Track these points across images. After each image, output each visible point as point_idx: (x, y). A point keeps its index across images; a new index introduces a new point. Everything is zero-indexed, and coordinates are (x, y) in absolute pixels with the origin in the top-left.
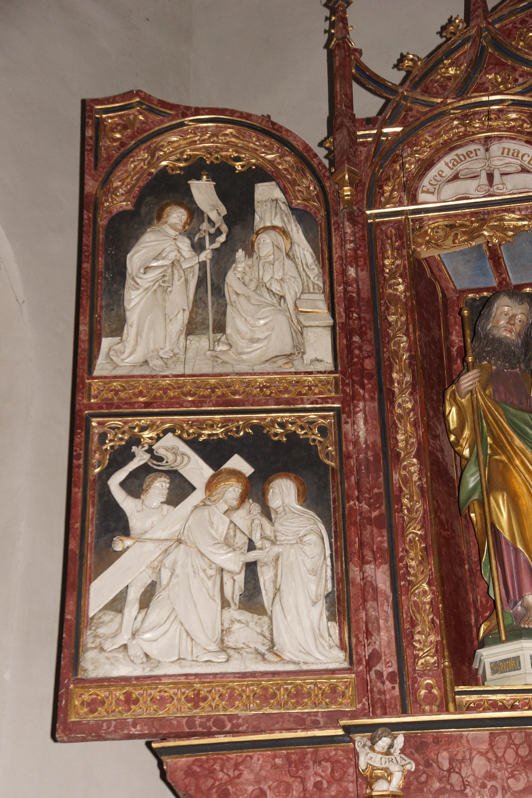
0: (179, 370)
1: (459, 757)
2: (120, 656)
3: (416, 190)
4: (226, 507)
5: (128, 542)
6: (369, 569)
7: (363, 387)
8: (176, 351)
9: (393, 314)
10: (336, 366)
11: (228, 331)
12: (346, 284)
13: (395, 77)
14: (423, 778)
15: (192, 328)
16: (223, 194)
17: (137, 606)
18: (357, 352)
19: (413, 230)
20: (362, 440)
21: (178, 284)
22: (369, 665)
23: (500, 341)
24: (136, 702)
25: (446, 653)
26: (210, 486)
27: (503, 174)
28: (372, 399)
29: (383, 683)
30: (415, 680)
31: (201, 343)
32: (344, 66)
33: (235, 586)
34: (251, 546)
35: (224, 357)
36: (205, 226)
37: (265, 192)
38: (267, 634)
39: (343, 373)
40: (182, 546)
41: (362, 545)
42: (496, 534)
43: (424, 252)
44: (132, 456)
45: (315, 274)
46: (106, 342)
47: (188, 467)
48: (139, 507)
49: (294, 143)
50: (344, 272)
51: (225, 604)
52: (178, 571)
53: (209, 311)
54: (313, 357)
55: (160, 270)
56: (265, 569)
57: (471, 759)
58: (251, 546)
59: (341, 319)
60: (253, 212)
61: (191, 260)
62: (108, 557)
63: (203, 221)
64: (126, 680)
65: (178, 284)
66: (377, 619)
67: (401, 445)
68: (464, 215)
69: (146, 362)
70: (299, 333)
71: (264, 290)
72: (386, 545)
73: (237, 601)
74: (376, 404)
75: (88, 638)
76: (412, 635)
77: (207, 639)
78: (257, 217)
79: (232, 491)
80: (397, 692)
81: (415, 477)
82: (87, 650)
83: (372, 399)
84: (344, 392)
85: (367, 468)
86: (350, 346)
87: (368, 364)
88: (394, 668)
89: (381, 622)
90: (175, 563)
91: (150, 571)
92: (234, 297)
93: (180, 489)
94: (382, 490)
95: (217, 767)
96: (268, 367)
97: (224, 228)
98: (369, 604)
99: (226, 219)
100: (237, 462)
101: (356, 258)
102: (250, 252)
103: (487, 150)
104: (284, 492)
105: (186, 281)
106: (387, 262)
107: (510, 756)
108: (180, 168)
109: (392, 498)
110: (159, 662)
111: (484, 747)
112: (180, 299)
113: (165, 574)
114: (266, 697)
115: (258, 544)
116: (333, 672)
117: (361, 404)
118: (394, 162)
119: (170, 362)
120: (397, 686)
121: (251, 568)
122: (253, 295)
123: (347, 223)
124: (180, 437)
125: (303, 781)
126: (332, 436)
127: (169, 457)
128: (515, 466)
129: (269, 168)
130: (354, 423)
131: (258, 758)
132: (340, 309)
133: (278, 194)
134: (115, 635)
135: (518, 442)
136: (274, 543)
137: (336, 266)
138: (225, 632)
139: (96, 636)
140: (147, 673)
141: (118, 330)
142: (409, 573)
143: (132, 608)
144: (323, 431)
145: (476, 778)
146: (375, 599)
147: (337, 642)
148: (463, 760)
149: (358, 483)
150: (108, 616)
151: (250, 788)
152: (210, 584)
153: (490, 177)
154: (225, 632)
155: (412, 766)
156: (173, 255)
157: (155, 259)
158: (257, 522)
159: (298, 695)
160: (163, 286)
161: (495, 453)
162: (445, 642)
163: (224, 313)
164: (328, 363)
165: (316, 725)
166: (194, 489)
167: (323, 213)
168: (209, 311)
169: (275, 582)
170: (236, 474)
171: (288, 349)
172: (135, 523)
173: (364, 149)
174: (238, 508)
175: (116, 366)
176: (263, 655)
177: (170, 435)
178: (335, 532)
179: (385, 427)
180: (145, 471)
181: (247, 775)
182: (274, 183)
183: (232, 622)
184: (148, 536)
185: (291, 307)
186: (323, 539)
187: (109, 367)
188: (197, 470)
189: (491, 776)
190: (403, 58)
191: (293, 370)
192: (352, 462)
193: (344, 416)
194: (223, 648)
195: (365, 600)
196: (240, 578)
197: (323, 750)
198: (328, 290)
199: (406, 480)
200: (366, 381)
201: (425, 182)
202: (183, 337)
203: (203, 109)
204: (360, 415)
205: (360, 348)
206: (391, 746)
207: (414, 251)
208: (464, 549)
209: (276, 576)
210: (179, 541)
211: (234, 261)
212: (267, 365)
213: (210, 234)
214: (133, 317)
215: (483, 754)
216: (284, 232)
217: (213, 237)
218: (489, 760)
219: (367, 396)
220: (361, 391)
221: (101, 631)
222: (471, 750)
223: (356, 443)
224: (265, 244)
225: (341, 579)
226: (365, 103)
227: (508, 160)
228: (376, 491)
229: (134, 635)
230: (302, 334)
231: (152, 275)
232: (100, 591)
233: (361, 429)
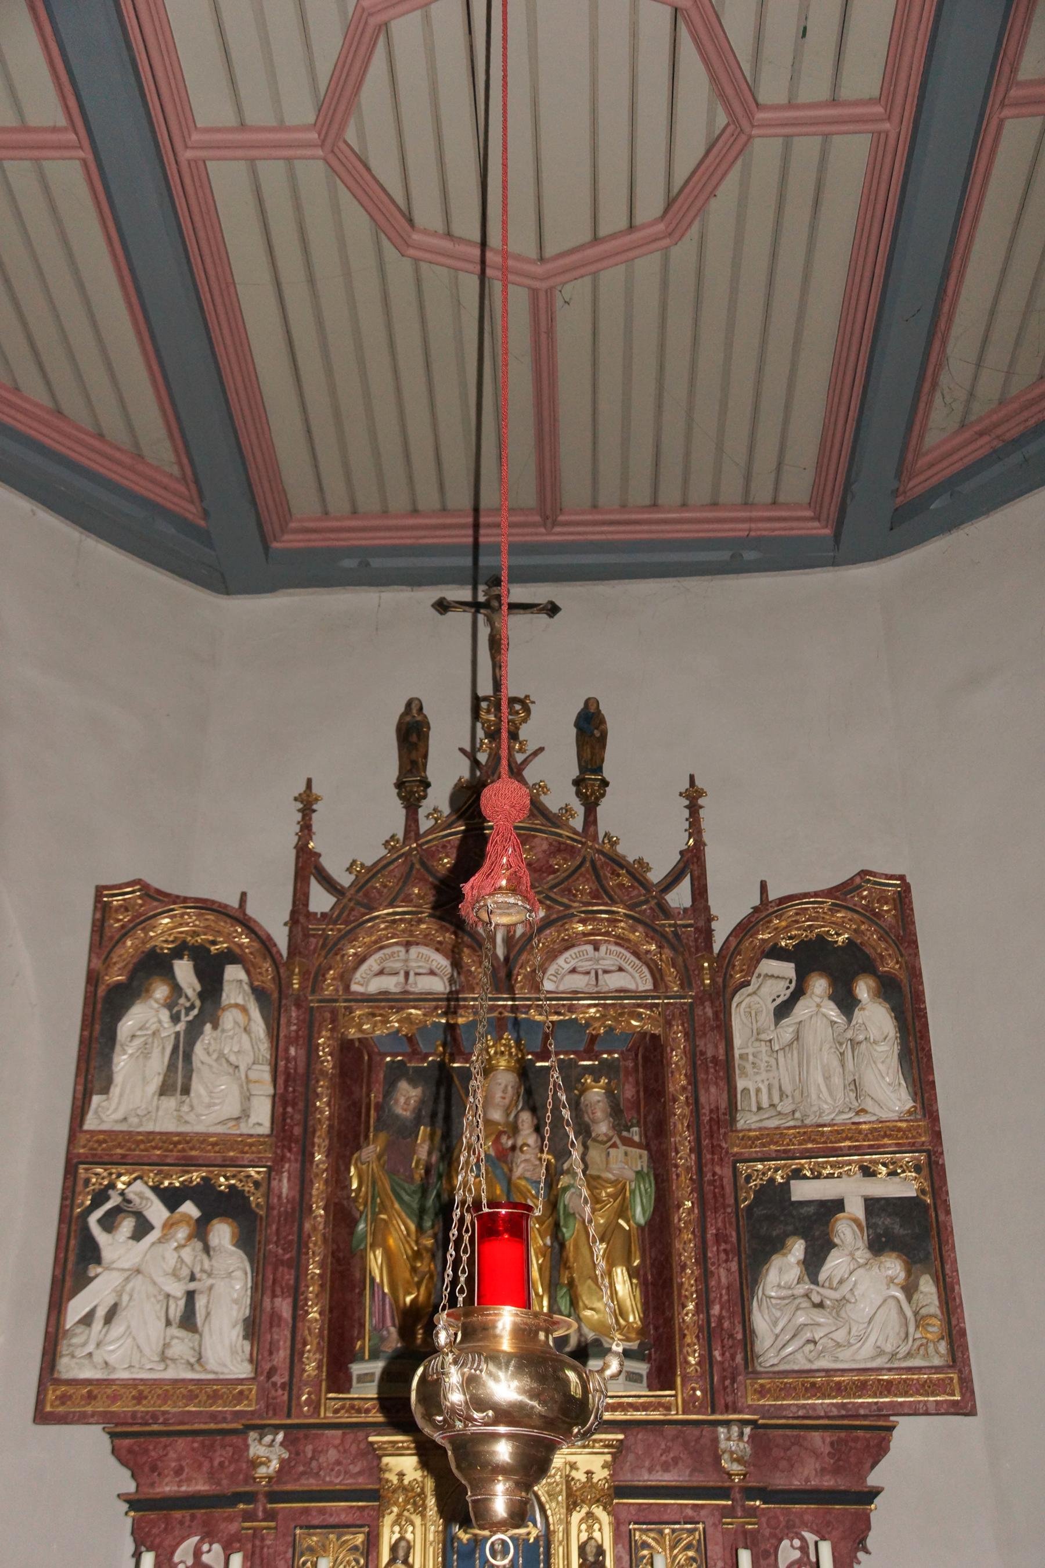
0: (149, 1127)
1: (320, 1449)
2: (86, 1362)
3: (350, 980)
4: (175, 1244)
5: (99, 1270)
6: (278, 1301)
7: (290, 1150)
8: (150, 1109)
9: (321, 1087)
10: (272, 1129)
11: (192, 1094)
12: (288, 1060)
13: (345, 880)
14: (293, 1464)
15: (165, 1090)
16: (199, 973)
17: (102, 1322)
18: (288, 1121)
19: (344, 1015)
20: (284, 1195)
21: (156, 1052)
22: (269, 1376)
23: (397, 1117)
24: (95, 1398)
25: (324, 1369)
26: (168, 1225)
27: (417, 974)
28: (296, 1160)
29: (276, 1391)
30: (300, 1389)
31: (170, 1103)
32: (307, 866)
33: (177, 1309)
34: (193, 1278)
35: (187, 1118)
36: (182, 1001)
37: (234, 973)
38: (197, 1348)
39: (276, 1137)
40: (140, 1277)
41: (274, 1281)
42: (373, 1279)
43: (352, 1033)
44: (108, 1198)
45: (264, 1048)
46: (96, 1099)
47: (151, 1209)
48: (110, 1241)
49: (260, 933)
50: (287, 1050)
51: (168, 1323)
52: (135, 1296)
53: (178, 1080)
54: (255, 1121)
55: (142, 1039)
56: (201, 1296)
57: (327, 1451)
58: (193, 1278)
59: (280, 1091)
60: (221, 990)
61: (169, 1030)
62: (83, 1281)
63: (180, 997)
64: (88, 1382)
65: (156, 1052)
66: (278, 1341)
67: (314, 1200)
68: (383, 1008)
69: (125, 1119)
70: (247, 1098)
71: (224, 1060)
72: (292, 1282)
73: (178, 1319)
74: (298, 1165)
75: (64, 1347)
76: (302, 1353)
77: (151, 1351)
78: (224, 995)
79: (182, 1233)
80: (286, 1397)
81: (321, 1227)
82: (61, 1357)
83: (296, 1160)
84: (275, 1153)
85: (285, 1219)
86: (285, 1113)
87: (297, 1131)
88: (286, 1379)
89: (281, 1343)
90: (133, 1290)
91: (114, 1294)
92: (199, 1065)
93: (143, 1227)
94: (295, 1238)
95: (151, 1447)
96: (220, 1129)
97: (198, 1003)
98: (274, 1329)
99: (201, 995)
100: (189, 1209)
101: (297, 1037)
102: (215, 1027)
103: (407, 951)
104: (222, 1233)
105: (164, 1048)
106: (321, 1041)
107: (354, 1449)
108: (168, 949)
109: (302, 1244)
110: (115, 1368)
111: (337, 1442)
112: (158, 1063)
113: (125, 1298)
114: (191, 1397)
115: (198, 1276)
116: (240, 1381)
117: (287, 1166)
118: (337, 954)
119: (144, 1119)
120: (286, 1393)
121: (190, 1295)
122: (214, 1064)
123: (293, 1008)
124: (146, 1183)
125: (211, 1460)
126: (263, 1189)
127: (137, 1200)
128: (393, 1225)
129: (237, 950)
130: (280, 1180)
131: (181, 1443)
132: (281, 1081)
133: (243, 976)
134: (84, 1345)
135: (397, 1206)
136: (210, 1275)
137: (282, 1044)
138: (166, 1346)
139: (70, 1345)
140: (105, 1377)
141: (105, 1090)
142: (306, 1305)
143: (98, 1324)
144: (257, 1184)
145: (328, 1465)
146: (279, 1326)
147: (248, 1356)
148: (321, 1452)
149: (278, 1230)
150: (80, 1329)
151: (173, 1464)
152: (158, 1307)
153: (407, 974)
154: (166, 1346)
155: (286, 1455)
156: (154, 1027)
157: (140, 1029)
158: (199, 1258)
159: (215, 1397)
160: (145, 1052)
161: (380, 1212)
162: (325, 1360)
163: (190, 1078)
164: (265, 1129)
165: (224, 1420)
166: (152, 1228)
167: (275, 995)
168: (178, 1080)
169: (207, 1307)
170: (186, 1218)
171: (236, 1114)
172: (107, 1254)
173: (313, 940)
174: (184, 1246)
175: (103, 1121)
176: (192, 1365)
177: (139, 1182)
178: (257, 1268)
179: (303, 1184)
180: (116, 1211)
181: (172, 1455)
182: (240, 966)
183: (173, 1338)
184: (115, 1266)
185: (243, 1077)
186: (246, 1274)
187: (96, 1122)
188: (157, 1212)
189: (338, 1463)
190: (354, 862)
191: (238, 1132)
192: (275, 1212)
193: (273, 1173)
194: (163, 1358)
195: (271, 1327)
196: (182, 1303)
197: (228, 1439)
198: (273, 1063)
199: (314, 1228)
200: (293, 1145)
201: (358, 975)
202: (156, 1097)
203: (191, 898)
204: (285, 1174)
205: (292, 1118)
206: (273, 1441)
207: (343, 1033)
208: (358, 1275)
209: (208, 1302)
210: (138, 1271)
211: (202, 1033)
212: (219, 1126)
213: (186, 1008)
214: (118, 1078)
215: (336, 1447)
216: (244, 1009)
217: (189, 1010)
218: (339, 1451)
219: (292, 1158)
220: (288, 1155)
221: (74, 1341)
222: (328, 1445)
223: (280, 1197)
224: (229, 1019)
225: (256, 1306)
226: (321, 901)
227: (420, 964)
228: (290, 1237)
229: (98, 1345)
230: (249, 1099)
231: (137, 1042)
232: (76, 1308)
233: (284, 1186)
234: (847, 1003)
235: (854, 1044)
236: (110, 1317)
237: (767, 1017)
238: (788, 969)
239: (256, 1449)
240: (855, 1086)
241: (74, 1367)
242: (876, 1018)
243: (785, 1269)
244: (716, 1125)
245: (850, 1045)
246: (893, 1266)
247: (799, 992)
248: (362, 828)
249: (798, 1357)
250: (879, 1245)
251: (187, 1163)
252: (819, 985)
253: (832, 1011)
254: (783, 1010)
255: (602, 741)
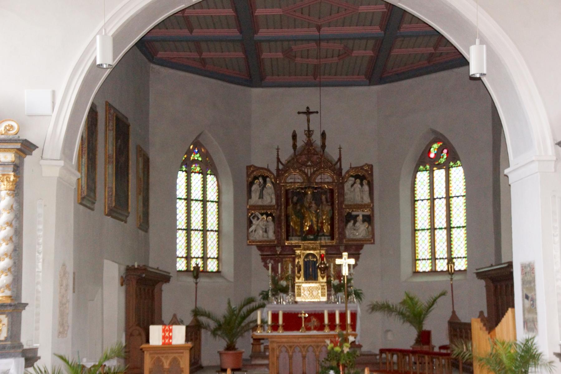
15: (259, 198)
31: (260, 200)
32: (279, 160)
33: (264, 230)
37: (268, 179)
45: (273, 191)
53: (261, 197)
61: (259, 189)
93: (258, 219)
112: (258, 194)
168: (261, 197)
172: (254, 222)
188: (260, 216)
232: (251, 230)
234: (362, 184)
235: (362, 191)
236: (255, 231)
237: (350, 186)
238: (353, 179)
239: (277, 249)
240: (362, 198)
241: (251, 238)
242: (366, 188)
243: (351, 224)
244: (341, 203)
245: (362, 191)
246: (366, 224)
247: (355, 183)
248: (286, 154)
249: (352, 237)
250: (364, 221)
251: (263, 209)
252: (358, 181)
253: (359, 186)
254: (352, 186)
255: (325, 139)
